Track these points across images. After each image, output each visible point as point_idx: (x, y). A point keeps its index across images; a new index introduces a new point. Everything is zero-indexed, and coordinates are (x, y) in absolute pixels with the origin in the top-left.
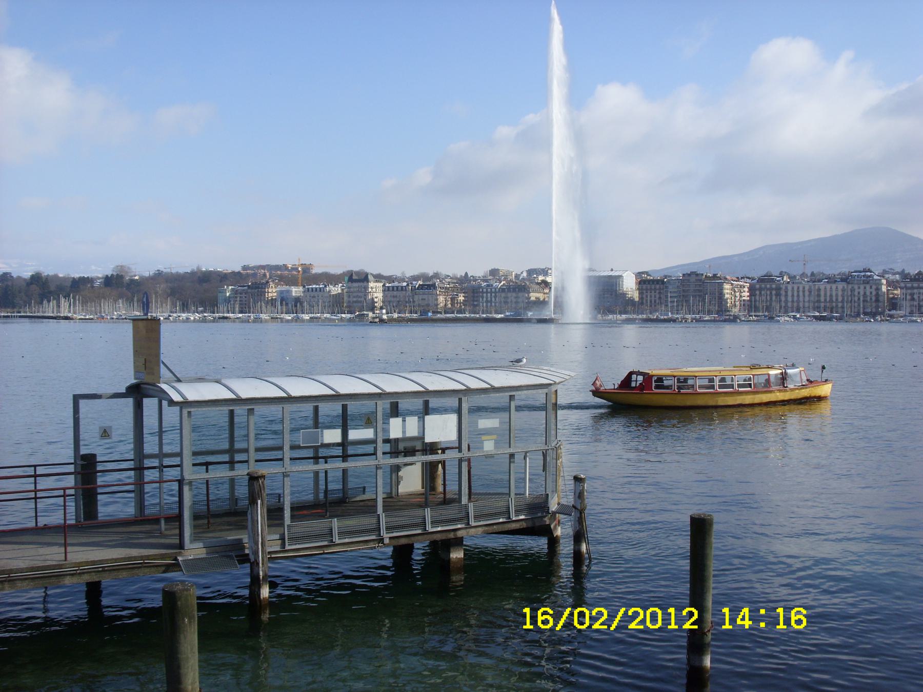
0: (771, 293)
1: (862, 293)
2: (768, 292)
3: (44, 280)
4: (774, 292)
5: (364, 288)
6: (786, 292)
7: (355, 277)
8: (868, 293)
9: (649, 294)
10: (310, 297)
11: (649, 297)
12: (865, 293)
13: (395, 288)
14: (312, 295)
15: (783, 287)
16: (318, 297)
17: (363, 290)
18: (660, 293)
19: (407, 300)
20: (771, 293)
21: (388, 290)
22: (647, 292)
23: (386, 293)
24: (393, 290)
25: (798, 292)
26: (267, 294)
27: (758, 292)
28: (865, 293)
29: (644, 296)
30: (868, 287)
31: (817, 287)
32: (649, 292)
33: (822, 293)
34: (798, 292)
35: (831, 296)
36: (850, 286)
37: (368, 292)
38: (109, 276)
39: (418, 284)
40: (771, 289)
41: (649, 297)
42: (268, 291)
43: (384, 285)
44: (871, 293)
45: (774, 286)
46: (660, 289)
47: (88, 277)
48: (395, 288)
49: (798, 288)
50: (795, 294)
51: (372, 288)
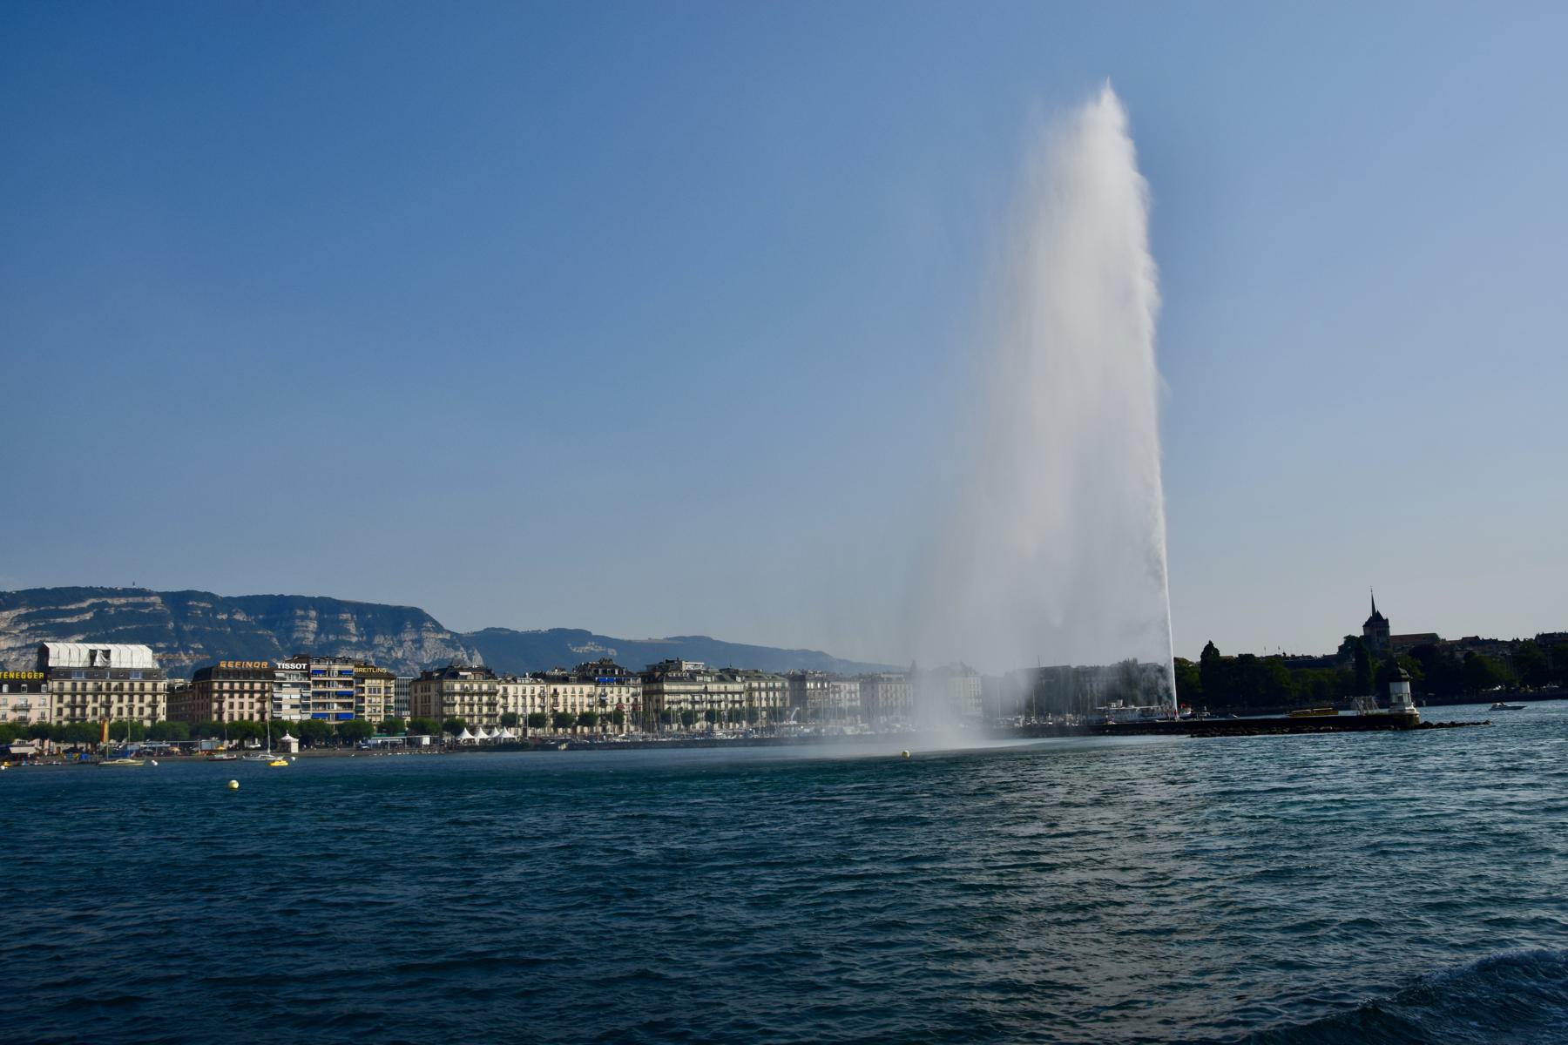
0: (480, 700)
1: (616, 701)
2: (476, 698)
4: (485, 699)
6: (505, 697)
8: (624, 701)
9: (236, 699)
11: (236, 706)
12: (620, 699)
15: (500, 688)
18: (262, 700)
20: (480, 700)
22: (232, 697)
25: (524, 698)
27: (457, 698)
28: (620, 699)
29: (226, 705)
30: (624, 690)
31: (552, 691)
32: (236, 695)
33: (561, 699)
34: (524, 698)
35: (573, 705)
36: (599, 690)
40: (481, 694)
41: (236, 706)
44: (628, 700)
45: (485, 687)
46: (263, 692)
49: (524, 691)
50: (520, 701)
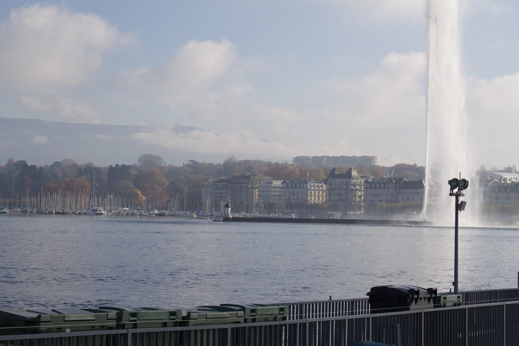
3: (38, 170)
5: (346, 185)
7: (336, 173)
10: (289, 194)
13: (378, 185)
14: (292, 192)
16: (298, 194)
17: (345, 187)
19: (390, 199)
21: (371, 188)
23: (368, 190)
24: (375, 187)
38: (114, 166)
43: (366, 182)
47: (117, 166)
48: (378, 185)
51: (355, 185)
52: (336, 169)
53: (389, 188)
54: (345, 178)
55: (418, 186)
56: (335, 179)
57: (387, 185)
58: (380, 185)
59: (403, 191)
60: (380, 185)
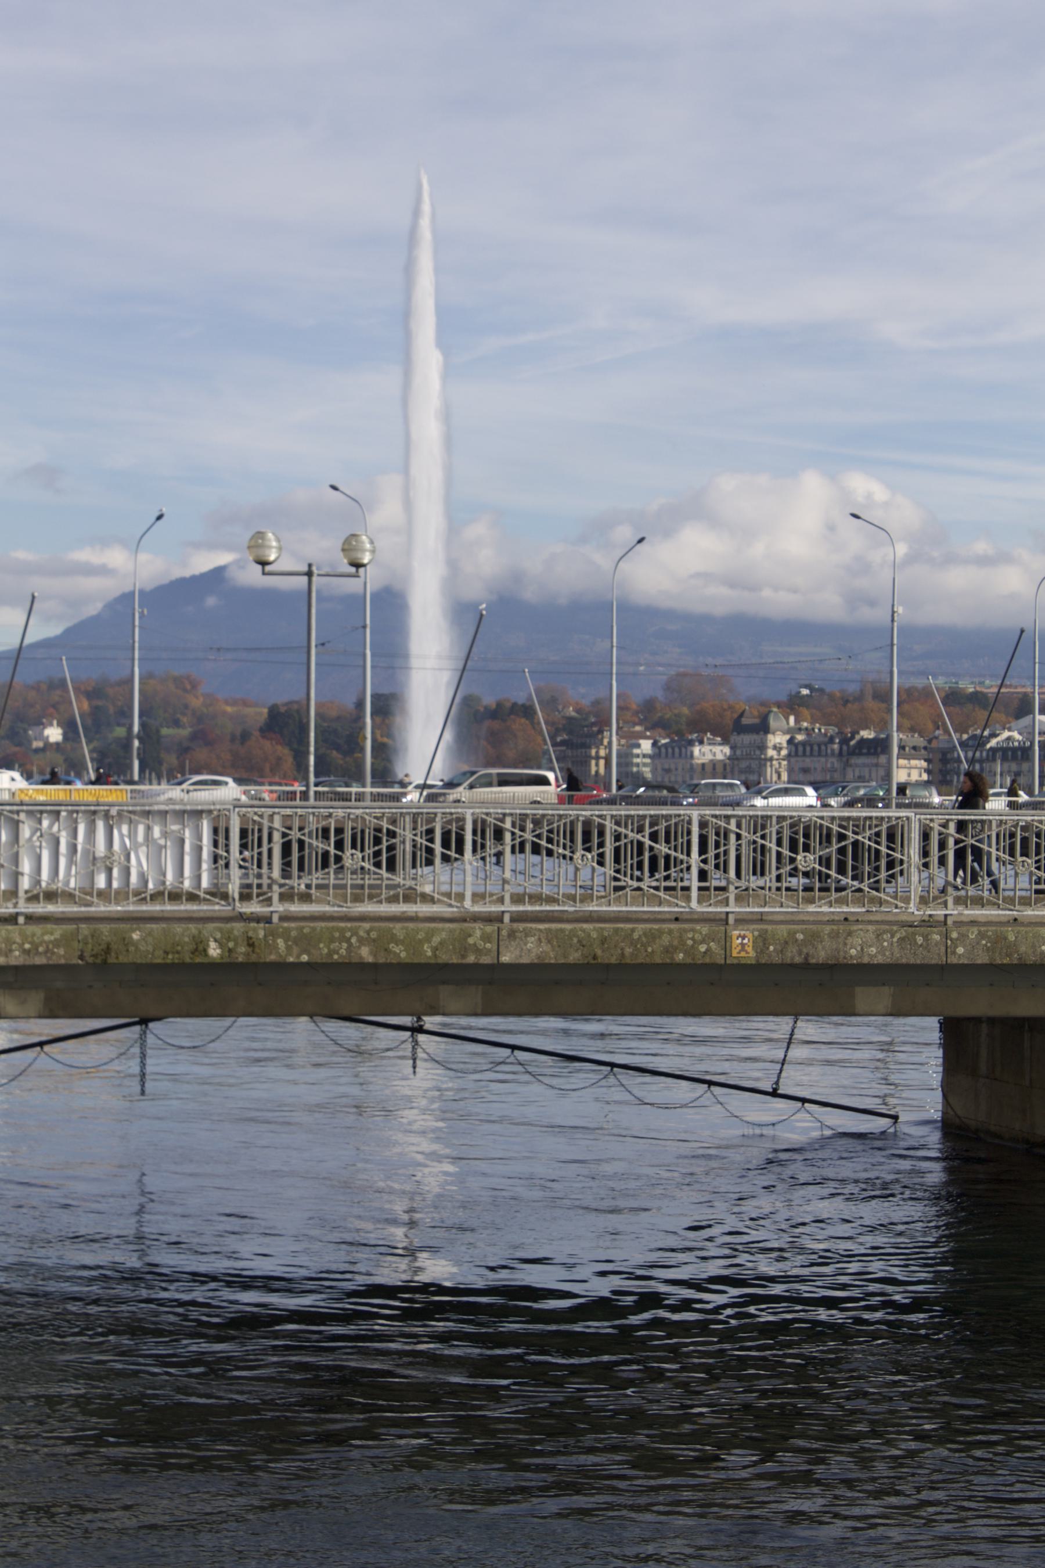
13: (808, 749)
21: (796, 755)
23: (793, 760)
24: (804, 754)
26: (593, 762)
37: (766, 760)
39: (858, 737)
42: (597, 752)
43: (790, 742)
48: (808, 749)
51: (777, 748)
52: (747, 714)
53: (826, 755)
54: (758, 733)
55: (879, 749)
56: (742, 736)
57: (823, 747)
58: (812, 750)
59: (854, 760)
60: (812, 750)
